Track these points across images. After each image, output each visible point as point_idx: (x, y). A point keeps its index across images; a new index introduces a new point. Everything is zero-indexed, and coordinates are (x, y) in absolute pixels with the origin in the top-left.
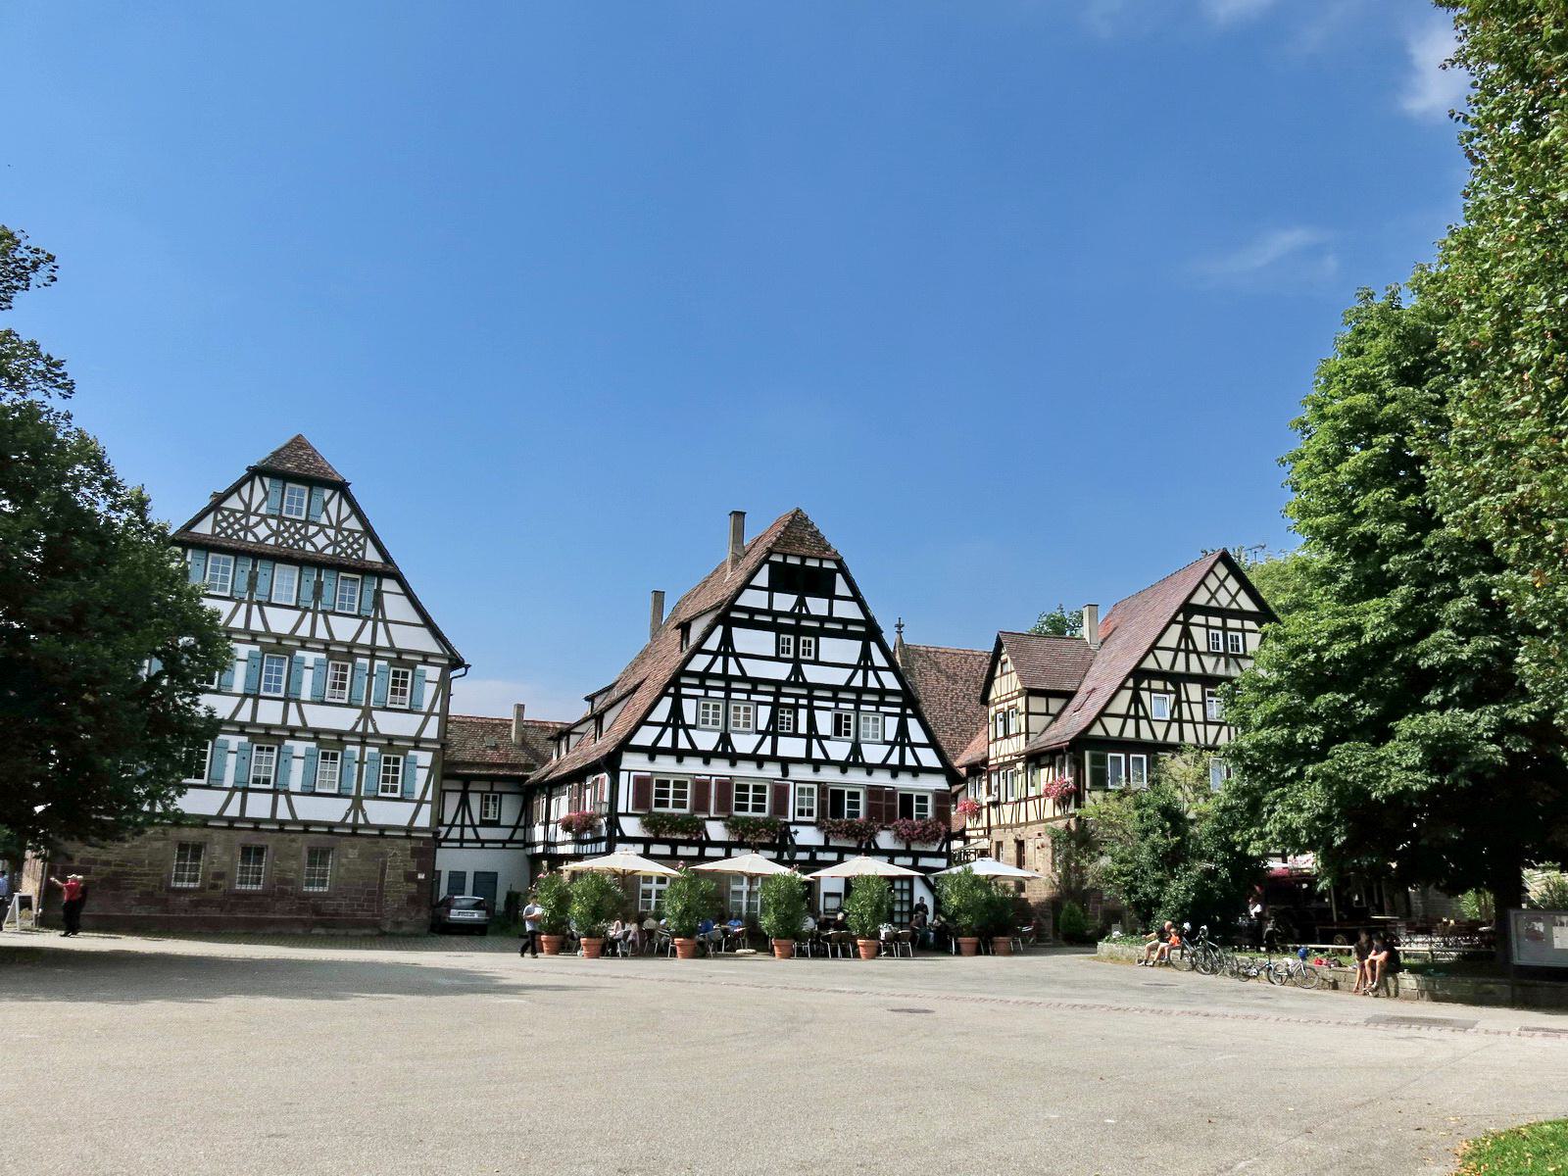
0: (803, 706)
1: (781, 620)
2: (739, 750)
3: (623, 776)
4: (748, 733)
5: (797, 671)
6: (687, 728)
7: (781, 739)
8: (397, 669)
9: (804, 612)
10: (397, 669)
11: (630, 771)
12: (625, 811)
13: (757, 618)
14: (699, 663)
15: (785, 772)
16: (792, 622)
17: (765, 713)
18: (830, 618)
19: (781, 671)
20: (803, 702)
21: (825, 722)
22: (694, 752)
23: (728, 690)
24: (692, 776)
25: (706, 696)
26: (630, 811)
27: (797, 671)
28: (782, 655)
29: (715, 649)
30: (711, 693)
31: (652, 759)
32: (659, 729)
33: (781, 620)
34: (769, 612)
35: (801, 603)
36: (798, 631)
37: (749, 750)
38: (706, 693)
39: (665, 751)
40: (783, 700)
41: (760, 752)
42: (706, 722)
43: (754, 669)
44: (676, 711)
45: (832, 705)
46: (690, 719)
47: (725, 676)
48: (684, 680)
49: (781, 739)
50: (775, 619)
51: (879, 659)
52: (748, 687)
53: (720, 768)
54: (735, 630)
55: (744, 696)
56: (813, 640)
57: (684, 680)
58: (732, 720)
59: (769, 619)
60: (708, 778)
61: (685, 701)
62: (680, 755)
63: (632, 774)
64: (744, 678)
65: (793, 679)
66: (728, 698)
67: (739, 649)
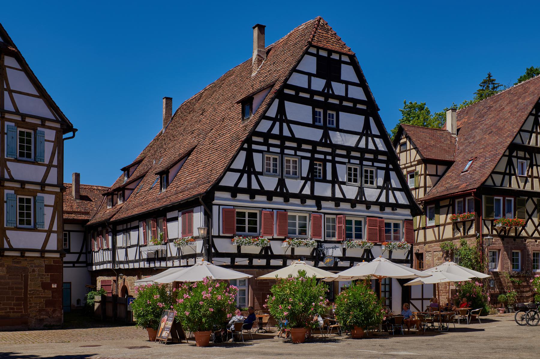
0: (329, 161)
1: (316, 98)
2: (291, 191)
3: (215, 209)
4: (296, 179)
5: (326, 135)
6: (257, 174)
7: (316, 184)
8: (23, 130)
9: (331, 92)
10: (23, 130)
11: (219, 205)
13: (301, 94)
14: (264, 126)
15: (319, 206)
16: (322, 99)
17: (306, 164)
18: (346, 98)
19: (316, 135)
20: (329, 157)
21: (342, 173)
22: (262, 192)
23: (282, 147)
24: (260, 209)
25: (268, 151)
26: (221, 234)
27: (326, 135)
28: (317, 124)
29: (274, 116)
30: (272, 149)
31: (234, 196)
32: (239, 174)
33: (316, 98)
34: (308, 90)
35: (328, 86)
36: (326, 106)
37: (297, 191)
38: (268, 149)
39: (243, 191)
40: (317, 156)
41: (304, 192)
42: (268, 170)
43: (300, 132)
44: (249, 161)
45: (346, 160)
46: (258, 167)
47: (281, 137)
48: (255, 139)
49: (316, 184)
50: (312, 97)
51: (375, 130)
52: (294, 145)
53: (278, 202)
54: (287, 104)
55: (292, 152)
56: (334, 113)
57: (255, 139)
58: (285, 169)
59: (307, 96)
60: (271, 210)
61: (255, 154)
62: (252, 193)
63: (221, 207)
64: (293, 139)
65: (323, 141)
66: (282, 153)
67: (289, 117)
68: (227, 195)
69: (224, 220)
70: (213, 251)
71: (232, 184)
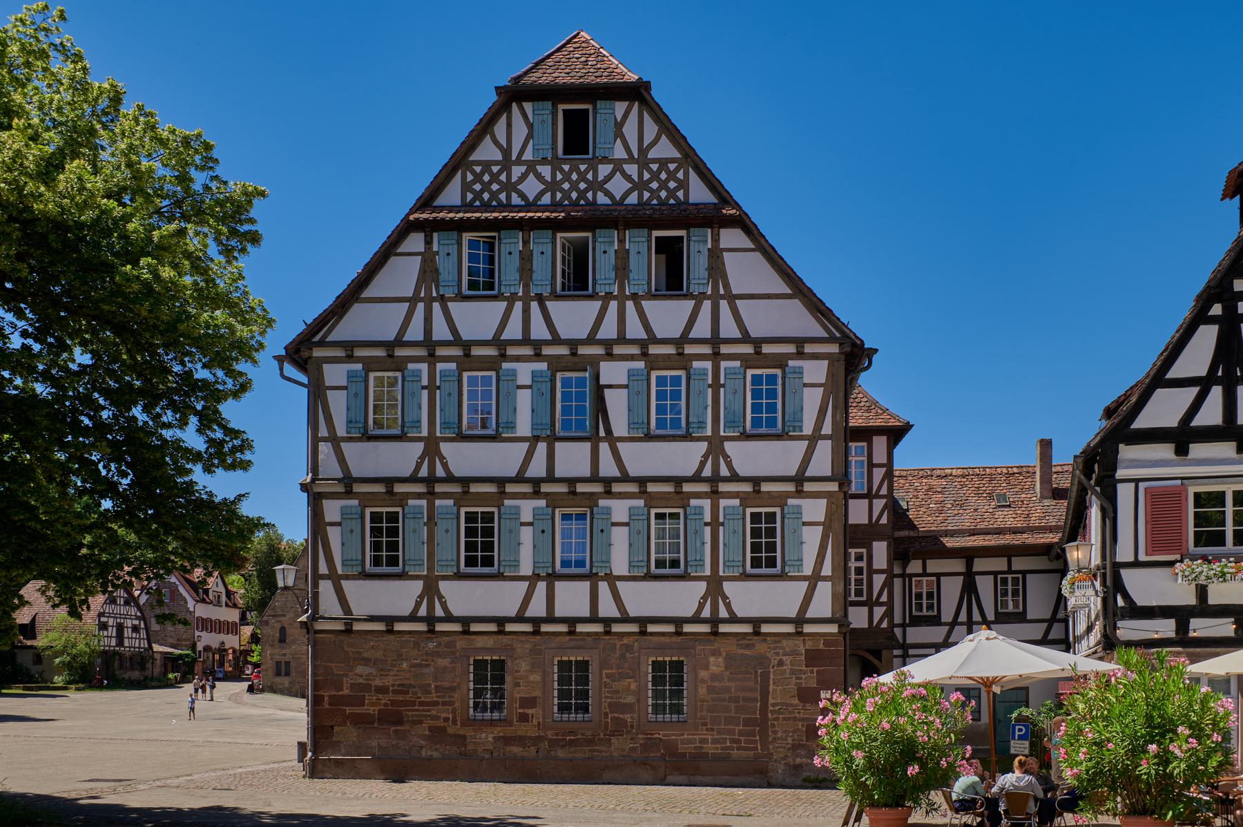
11: (1137, 481)
12: (1131, 559)
26: (1143, 557)
31: (1182, 451)
39: (1209, 434)
63: (1142, 485)
68: (1165, 451)
69: (1149, 518)
70: (1120, 602)
71: (1171, 420)
